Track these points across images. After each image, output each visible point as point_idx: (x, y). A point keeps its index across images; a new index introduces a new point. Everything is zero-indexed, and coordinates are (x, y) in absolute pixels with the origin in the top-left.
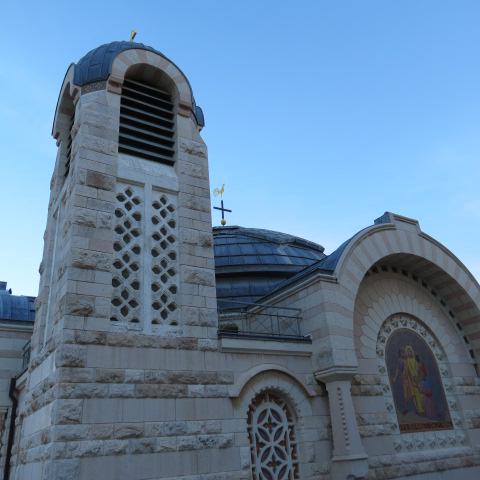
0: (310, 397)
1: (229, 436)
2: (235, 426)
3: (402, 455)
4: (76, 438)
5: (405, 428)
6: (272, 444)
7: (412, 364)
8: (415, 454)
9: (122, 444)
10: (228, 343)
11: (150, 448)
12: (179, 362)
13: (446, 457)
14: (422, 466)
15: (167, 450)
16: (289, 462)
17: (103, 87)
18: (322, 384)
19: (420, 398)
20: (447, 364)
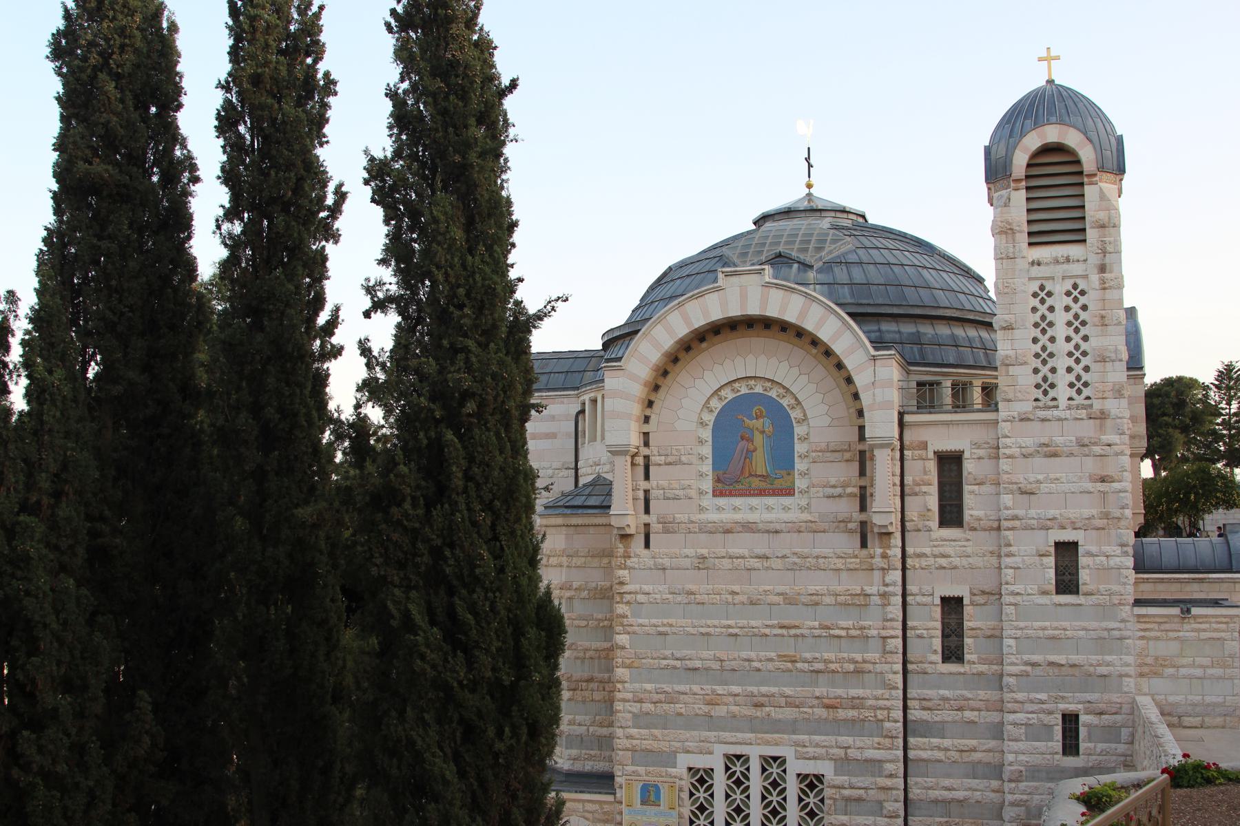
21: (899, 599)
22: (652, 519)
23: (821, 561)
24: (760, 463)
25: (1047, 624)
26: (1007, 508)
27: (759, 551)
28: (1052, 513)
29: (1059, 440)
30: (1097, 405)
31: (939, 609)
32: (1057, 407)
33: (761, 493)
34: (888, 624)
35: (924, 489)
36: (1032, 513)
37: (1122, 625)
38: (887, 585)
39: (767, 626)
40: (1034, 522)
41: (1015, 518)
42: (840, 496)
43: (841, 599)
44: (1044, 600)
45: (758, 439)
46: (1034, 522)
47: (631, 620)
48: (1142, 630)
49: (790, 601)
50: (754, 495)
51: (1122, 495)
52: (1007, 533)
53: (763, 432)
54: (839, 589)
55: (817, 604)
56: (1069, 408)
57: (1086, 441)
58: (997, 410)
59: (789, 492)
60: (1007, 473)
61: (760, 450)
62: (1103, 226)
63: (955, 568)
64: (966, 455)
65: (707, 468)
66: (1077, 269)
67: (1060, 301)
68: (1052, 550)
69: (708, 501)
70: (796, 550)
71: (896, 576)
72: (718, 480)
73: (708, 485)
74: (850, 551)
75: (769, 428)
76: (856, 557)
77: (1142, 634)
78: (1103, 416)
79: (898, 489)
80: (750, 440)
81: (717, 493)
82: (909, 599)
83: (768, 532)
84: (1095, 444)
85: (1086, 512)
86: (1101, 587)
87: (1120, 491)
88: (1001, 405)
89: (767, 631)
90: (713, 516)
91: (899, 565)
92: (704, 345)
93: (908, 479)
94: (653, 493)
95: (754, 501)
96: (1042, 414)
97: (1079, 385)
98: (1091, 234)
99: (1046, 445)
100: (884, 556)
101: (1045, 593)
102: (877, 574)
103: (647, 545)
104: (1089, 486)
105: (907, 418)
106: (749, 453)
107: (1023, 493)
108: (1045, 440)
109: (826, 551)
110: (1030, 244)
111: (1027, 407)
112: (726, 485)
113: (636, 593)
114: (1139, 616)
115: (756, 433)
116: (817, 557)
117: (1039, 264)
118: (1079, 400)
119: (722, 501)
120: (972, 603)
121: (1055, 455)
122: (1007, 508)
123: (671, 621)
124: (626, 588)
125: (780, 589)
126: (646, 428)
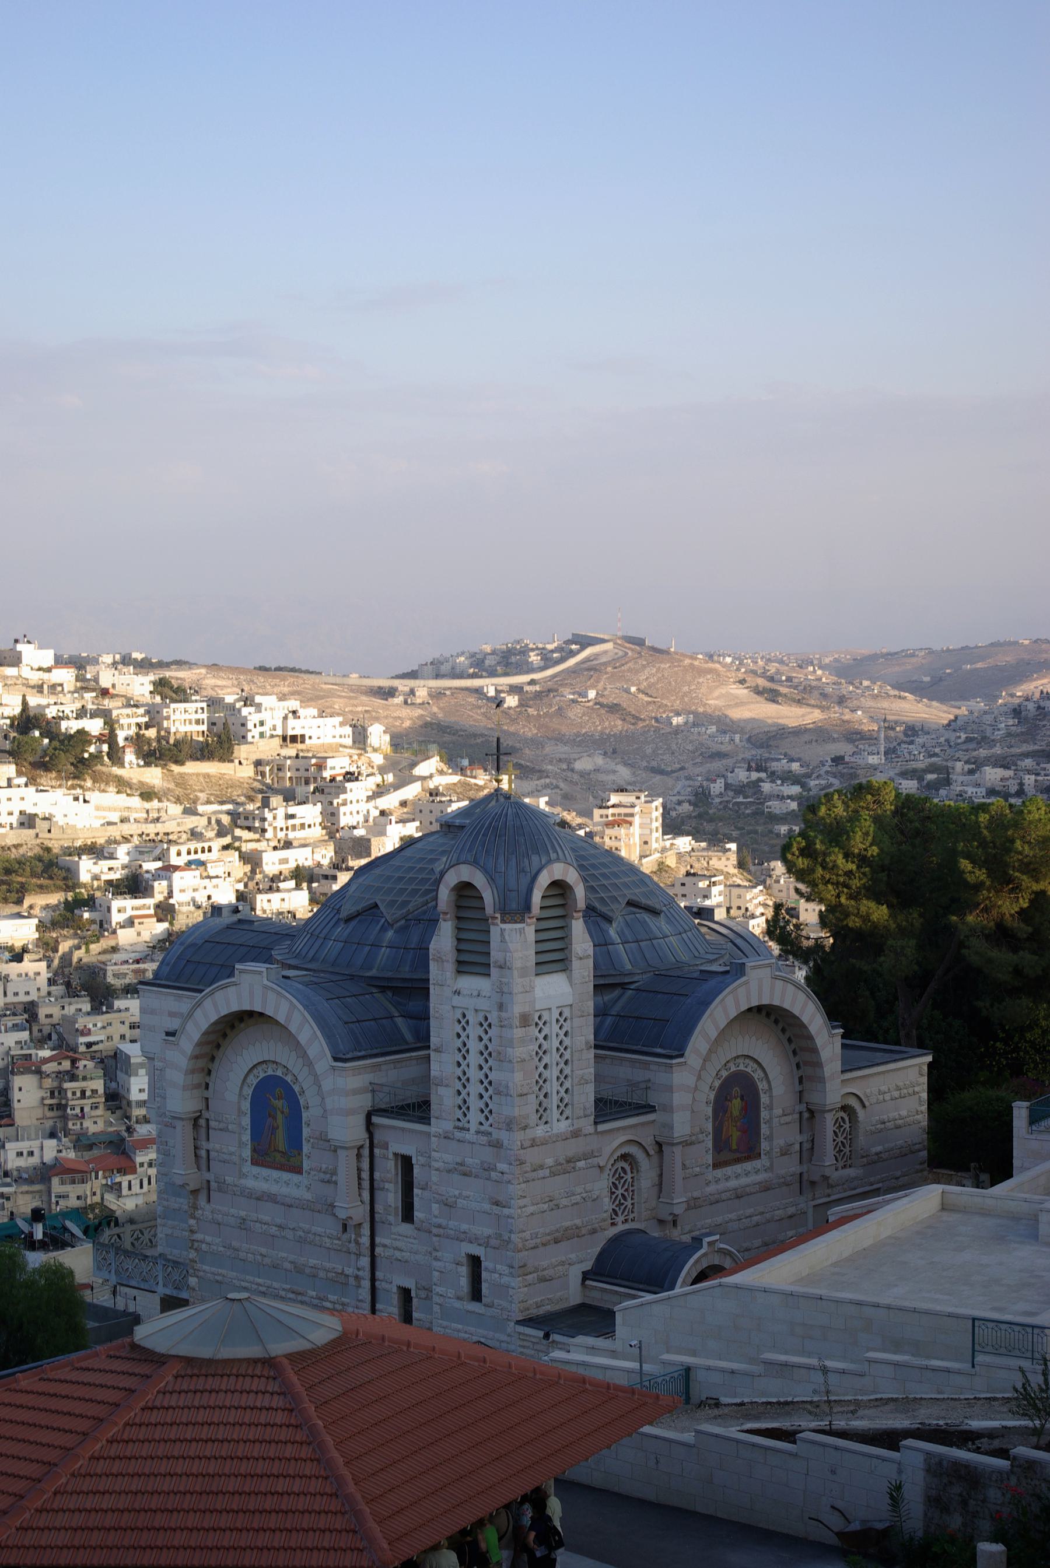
0: (648, 1154)
1: (597, 1193)
2: (601, 1185)
3: (712, 1189)
4: (525, 1206)
5: (716, 1165)
6: (620, 1191)
7: (736, 1105)
8: (721, 1186)
9: (546, 1206)
10: (601, 1127)
11: (557, 1206)
12: (573, 1148)
13: (747, 1186)
14: (724, 1196)
15: (566, 1206)
16: (629, 1202)
17: (522, 921)
18: (659, 1145)
19: (736, 1135)
20: (771, 1097)
21: (366, 1284)
22: (210, 1176)
23: (318, 1238)
24: (281, 1140)
25: (460, 1327)
26: (436, 1217)
27: (278, 1221)
28: (464, 1227)
29: (469, 1161)
30: (496, 1134)
31: (396, 1297)
32: (468, 1130)
33: (281, 1168)
34: (359, 1304)
35: (387, 1185)
36: (452, 1224)
37: (508, 1339)
38: (358, 1269)
39: (284, 1289)
40: (452, 1232)
41: (440, 1226)
42: (328, 1182)
43: (330, 1275)
44: (458, 1304)
45: (280, 1116)
46: (452, 1232)
47: (198, 1266)
48: (520, 1346)
49: (299, 1270)
50: (277, 1169)
51: (510, 1220)
52: (435, 1239)
53: (282, 1112)
54: (328, 1265)
55: (314, 1276)
56: (478, 1132)
57: (486, 1166)
58: (430, 1124)
59: (298, 1170)
60: (436, 1184)
61: (281, 1128)
62: (501, 967)
63: (406, 1262)
64: (414, 1161)
65: (247, 1137)
66: (483, 1004)
67: (474, 1031)
68: (464, 1260)
69: (248, 1168)
70: (301, 1225)
71: (365, 1262)
72: (254, 1150)
73: (247, 1153)
74: (335, 1233)
75: (286, 1110)
76: (339, 1239)
77: (522, 1350)
78: (497, 1145)
79: (366, 1184)
80: (275, 1118)
81: (255, 1162)
82: (377, 1283)
83: (283, 1204)
84: (493, 1170)
85: (488, 1231)
86: (496, 1301)
87: (508, 1217)
88: (433, 1120)
89: (283, 1293)
90: (250, 1183)
91: (368, 1252)
92: (242, 1025)
93: (377, 1175)
94: (212, 1154)
95: (275, 1174)
96: (459, 1135)
97: (486, 1111)
98: (494, 971)
99: (461, 1164)
100: (357, 1243)
101: (459, 1298)
102: (353, 1257)
103: (209, 1201)
104: (487, 1206)
105: (375, 1119)
106: (274, 1129)
107: (446, 1205)
108: (459, 1160)
109: (320, 1230)
110: (459, 972)
111: (448, 1126)
112: (262, 1156)
113: (202, 1242)
114: (520, 1333)
115: (279, 1113)
116: (315, 1234)
117: (459, 993)
118: (486, 1127)
119: (256, 1170)
120: (417, 1296)
121: (465, 1174)
122: (436, 1217)
123: (224, 1272)
124: (199, 1236)
125: (292, 1257)
126: (206, 1094)
